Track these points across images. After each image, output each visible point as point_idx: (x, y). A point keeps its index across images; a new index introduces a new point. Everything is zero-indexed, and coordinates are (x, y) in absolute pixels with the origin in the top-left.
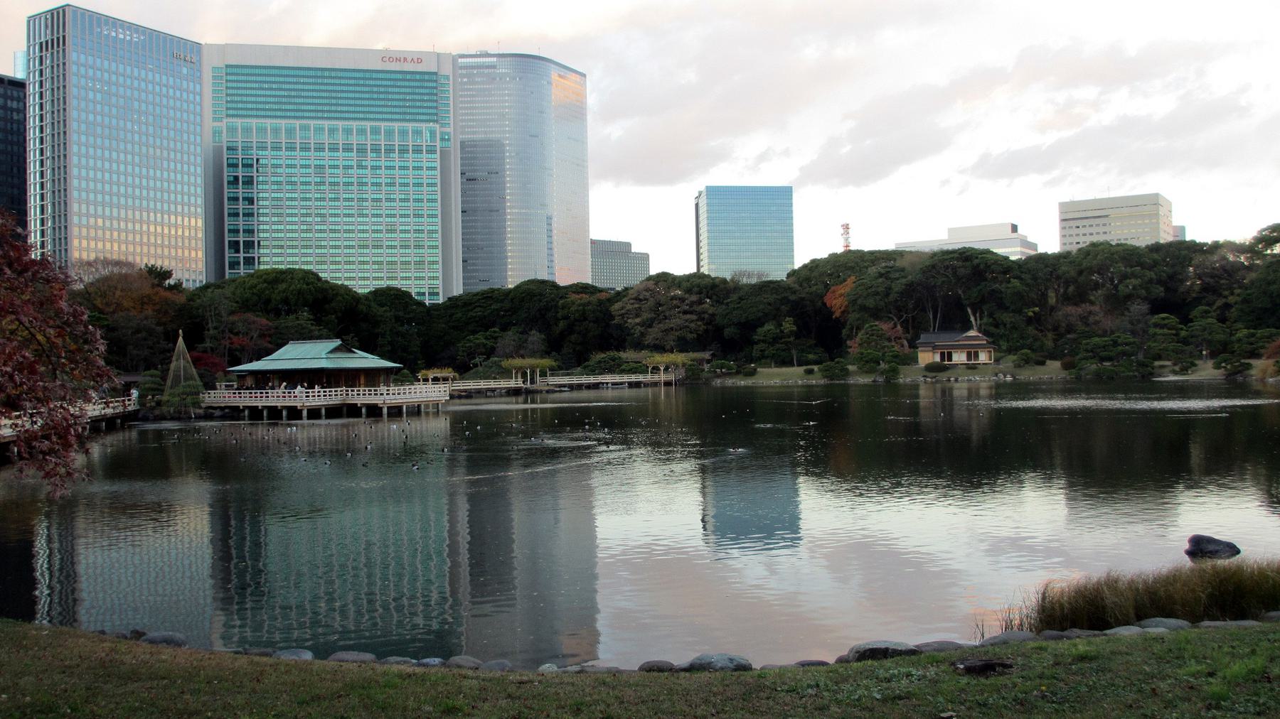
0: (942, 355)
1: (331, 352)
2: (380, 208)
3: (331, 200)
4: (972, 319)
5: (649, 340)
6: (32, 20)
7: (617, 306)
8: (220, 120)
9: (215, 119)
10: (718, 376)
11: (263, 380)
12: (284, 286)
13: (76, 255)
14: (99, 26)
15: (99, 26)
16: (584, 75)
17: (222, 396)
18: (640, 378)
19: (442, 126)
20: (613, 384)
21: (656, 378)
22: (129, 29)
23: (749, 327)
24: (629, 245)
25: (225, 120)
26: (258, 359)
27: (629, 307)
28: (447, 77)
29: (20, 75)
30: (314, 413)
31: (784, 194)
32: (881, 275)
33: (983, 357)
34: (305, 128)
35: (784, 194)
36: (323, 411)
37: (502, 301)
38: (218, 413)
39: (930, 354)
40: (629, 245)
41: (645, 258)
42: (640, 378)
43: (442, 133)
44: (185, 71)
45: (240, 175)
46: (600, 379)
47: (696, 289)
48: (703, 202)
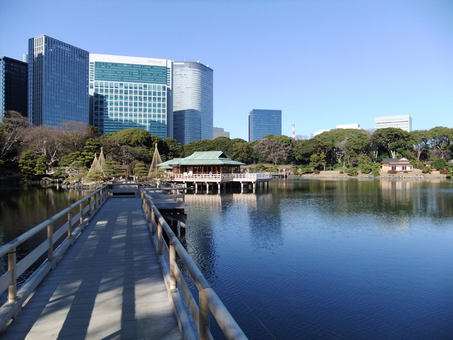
0: (393, 167)
4: (392, 154)
5: (268, 160)
7: (255, 146)
8: (93, 81)
12: (136, 135)
14: (54, 44)
15: (54, 44)
16: (212, 70)
19: (167, 85)
23: (308, 155)
25: (94, 81)
27: (260, 147)
28: (169, 69)
31: (279, 113)
33: (408, 169)
34: (121, 85)
35: (279, 113)
37: (210, 144)
44: (83, 61)
45: (99, 100)
47: (284, 141)
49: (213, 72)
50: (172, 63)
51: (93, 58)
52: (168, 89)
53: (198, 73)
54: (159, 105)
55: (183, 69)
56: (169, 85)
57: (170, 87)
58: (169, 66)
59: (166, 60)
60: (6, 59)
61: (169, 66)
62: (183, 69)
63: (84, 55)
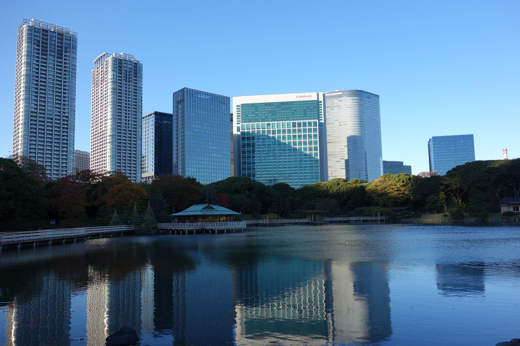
1: (204, 208)
2: (286, 153)
3: (278, 150)
6: (175, 94)
8: (239, 124)
9: (238, 124)
10: (405, 218)
11: (183, 219)
13: (187, 173)
15: (195, 94)
16: (378, 96)
17: (164, 226)
18: (369, 218)
20: (355, 221)
21: (376, 218)
22: (205, 94)
24: (402, 163)
26: (181, 211)
28: (321, 102)
29: (172, 113)
30: (191, 232)
31: (470, 138)
32: (486, 172)
35: (470, 138)
36: (195, 231)
38: (161, 231)
39: (507, 208)
40: (402, 163)
41: (409, 168)
42: (369, 218)
43: (319, 123)
44: (224, 107)
46: (350, 219)
48: (431, 143)
49: (379, 99)
50: (324, 95)
51: (236, 102)
52: (320, 124)
53: (356, 101)
54: (310, 143)
55: (341, 99)
56: (322, 120)
57: (323, 121)
58: (321, 99)
59: (316, 94)
60: (156, 113)
61: (321, 99)
62: (341, 99)
63: (225, 101)
